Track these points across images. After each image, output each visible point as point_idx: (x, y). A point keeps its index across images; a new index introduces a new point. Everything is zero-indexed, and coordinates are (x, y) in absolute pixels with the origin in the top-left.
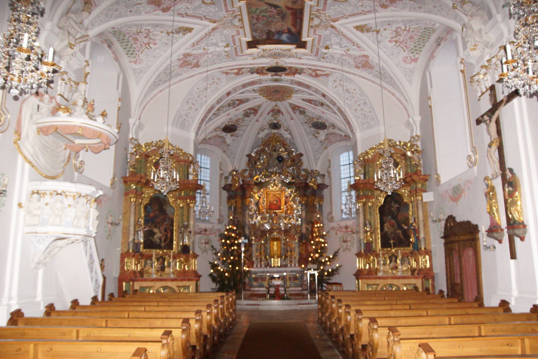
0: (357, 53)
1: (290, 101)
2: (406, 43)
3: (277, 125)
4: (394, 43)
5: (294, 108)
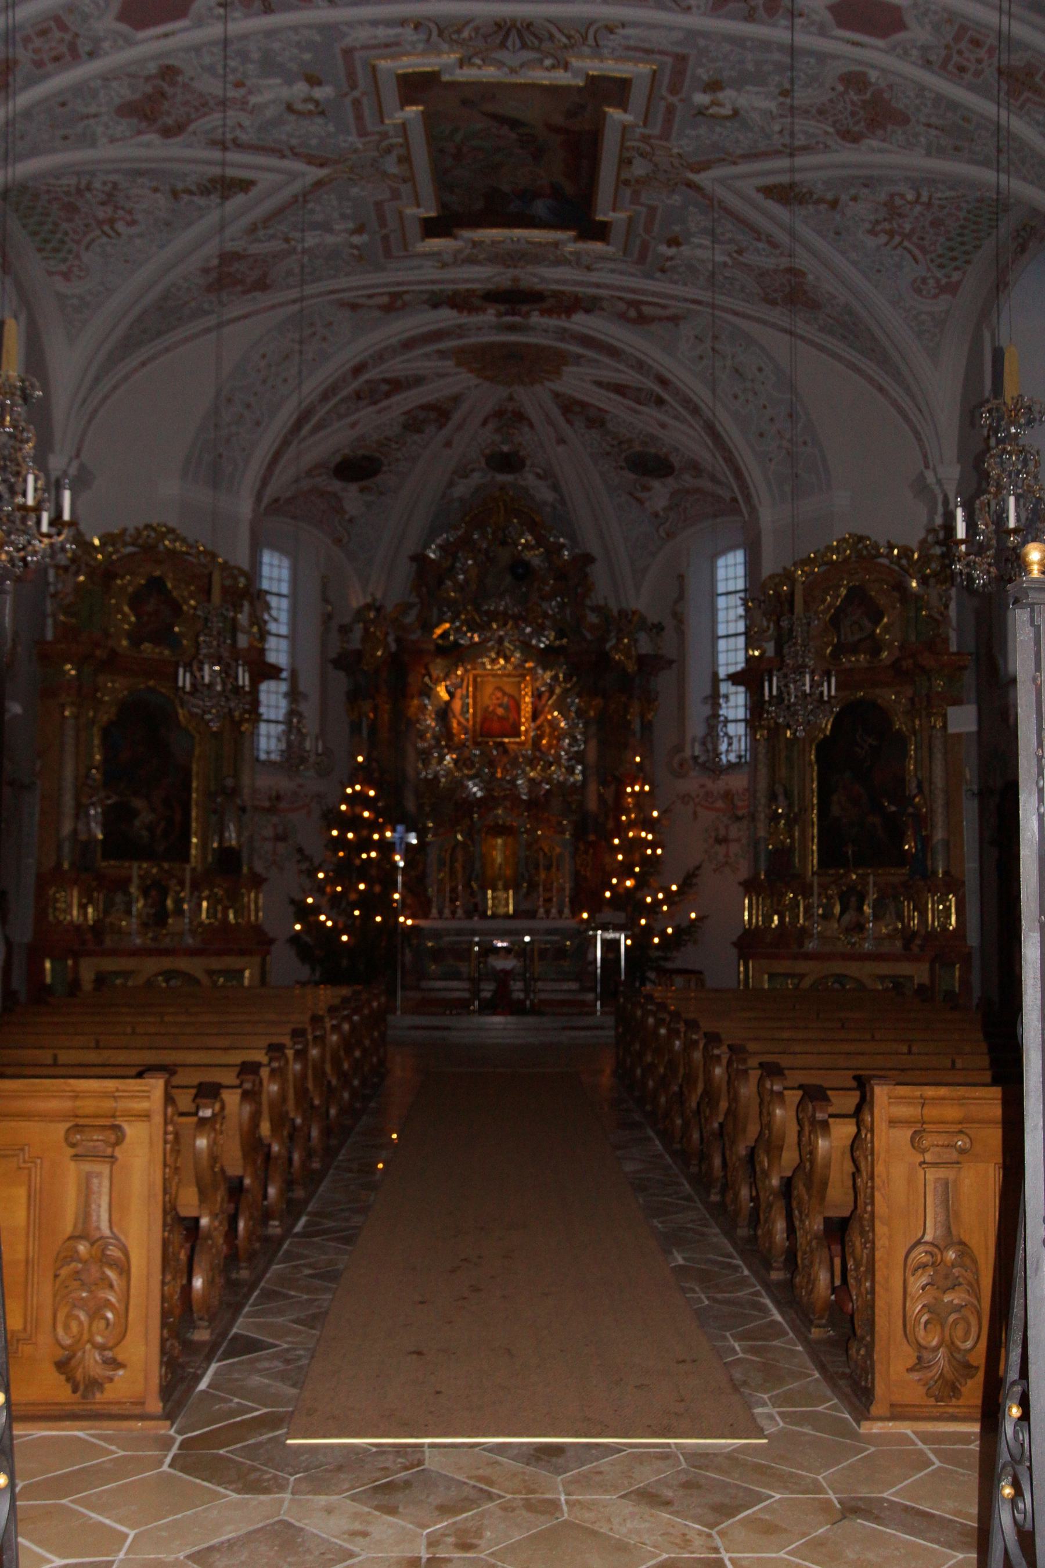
0: (769, 262)
1: (557, 386)
2: (922, 239)
4: (883, 238)
5: (570, 407)
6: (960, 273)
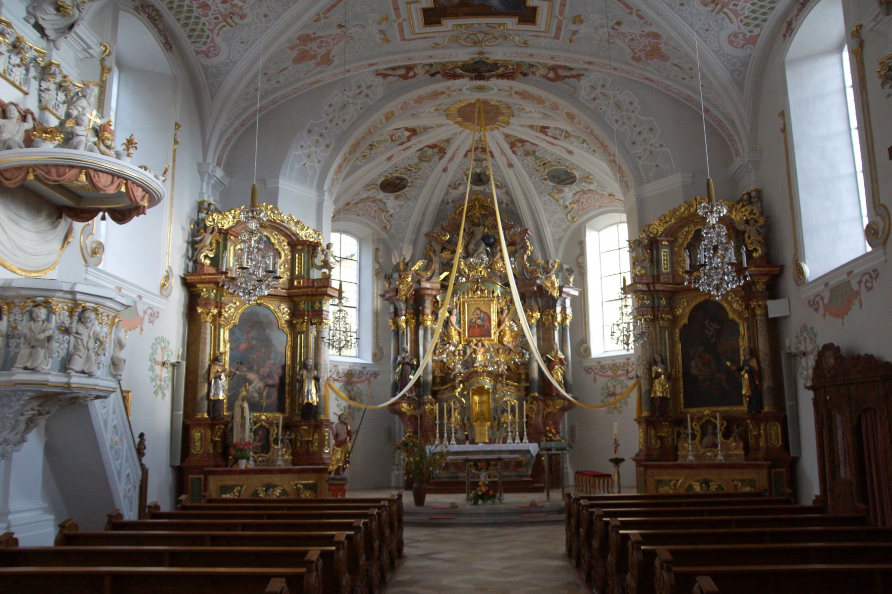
1: (507, 130)
3: (483, 177)
5: (515, 143)
6: (759, 29)
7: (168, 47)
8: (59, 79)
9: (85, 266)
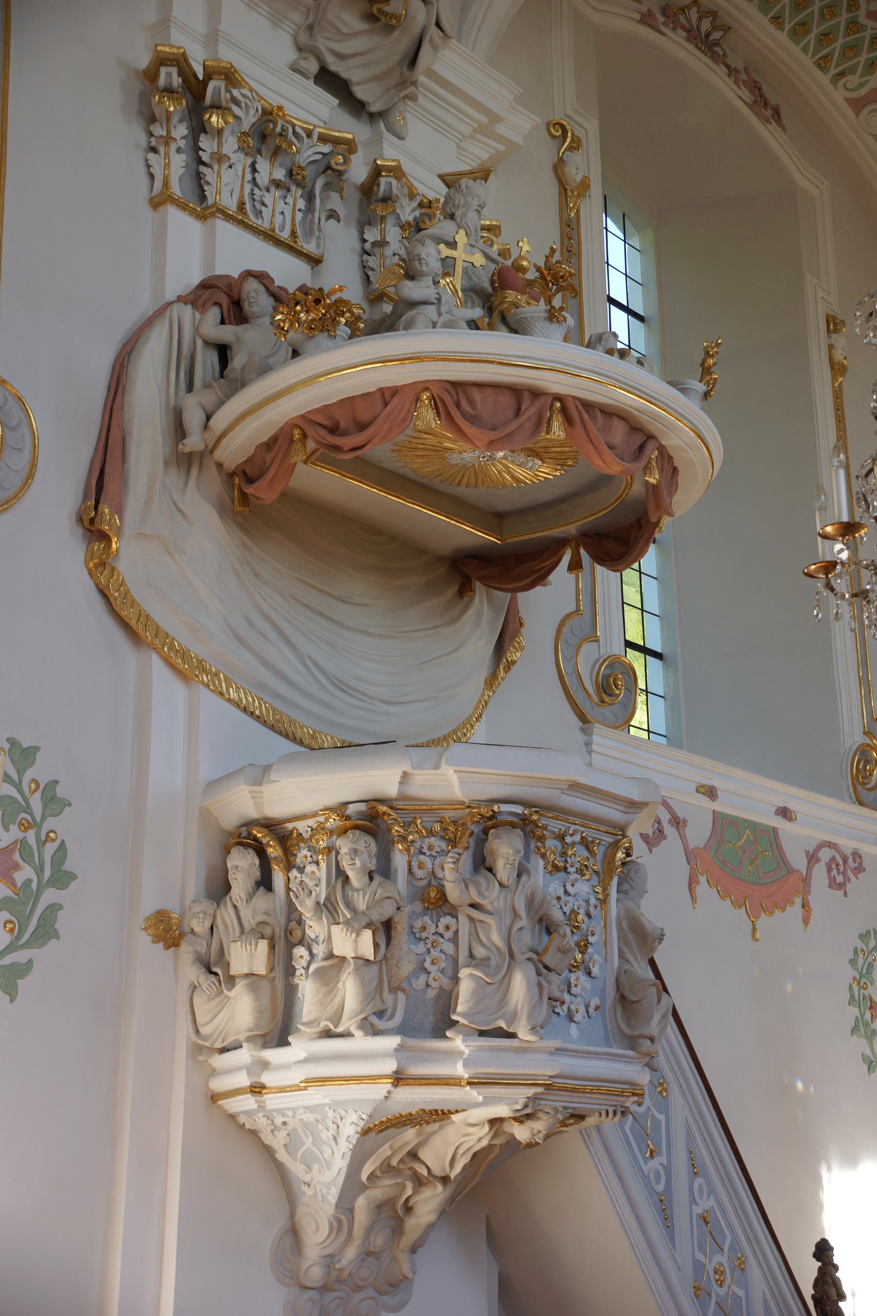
7: (768, 113)
8: (408, 212)
9: (583, 730)
